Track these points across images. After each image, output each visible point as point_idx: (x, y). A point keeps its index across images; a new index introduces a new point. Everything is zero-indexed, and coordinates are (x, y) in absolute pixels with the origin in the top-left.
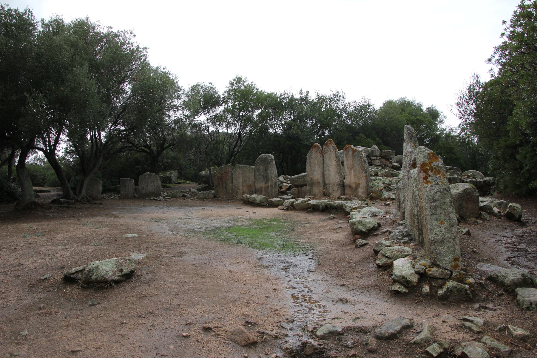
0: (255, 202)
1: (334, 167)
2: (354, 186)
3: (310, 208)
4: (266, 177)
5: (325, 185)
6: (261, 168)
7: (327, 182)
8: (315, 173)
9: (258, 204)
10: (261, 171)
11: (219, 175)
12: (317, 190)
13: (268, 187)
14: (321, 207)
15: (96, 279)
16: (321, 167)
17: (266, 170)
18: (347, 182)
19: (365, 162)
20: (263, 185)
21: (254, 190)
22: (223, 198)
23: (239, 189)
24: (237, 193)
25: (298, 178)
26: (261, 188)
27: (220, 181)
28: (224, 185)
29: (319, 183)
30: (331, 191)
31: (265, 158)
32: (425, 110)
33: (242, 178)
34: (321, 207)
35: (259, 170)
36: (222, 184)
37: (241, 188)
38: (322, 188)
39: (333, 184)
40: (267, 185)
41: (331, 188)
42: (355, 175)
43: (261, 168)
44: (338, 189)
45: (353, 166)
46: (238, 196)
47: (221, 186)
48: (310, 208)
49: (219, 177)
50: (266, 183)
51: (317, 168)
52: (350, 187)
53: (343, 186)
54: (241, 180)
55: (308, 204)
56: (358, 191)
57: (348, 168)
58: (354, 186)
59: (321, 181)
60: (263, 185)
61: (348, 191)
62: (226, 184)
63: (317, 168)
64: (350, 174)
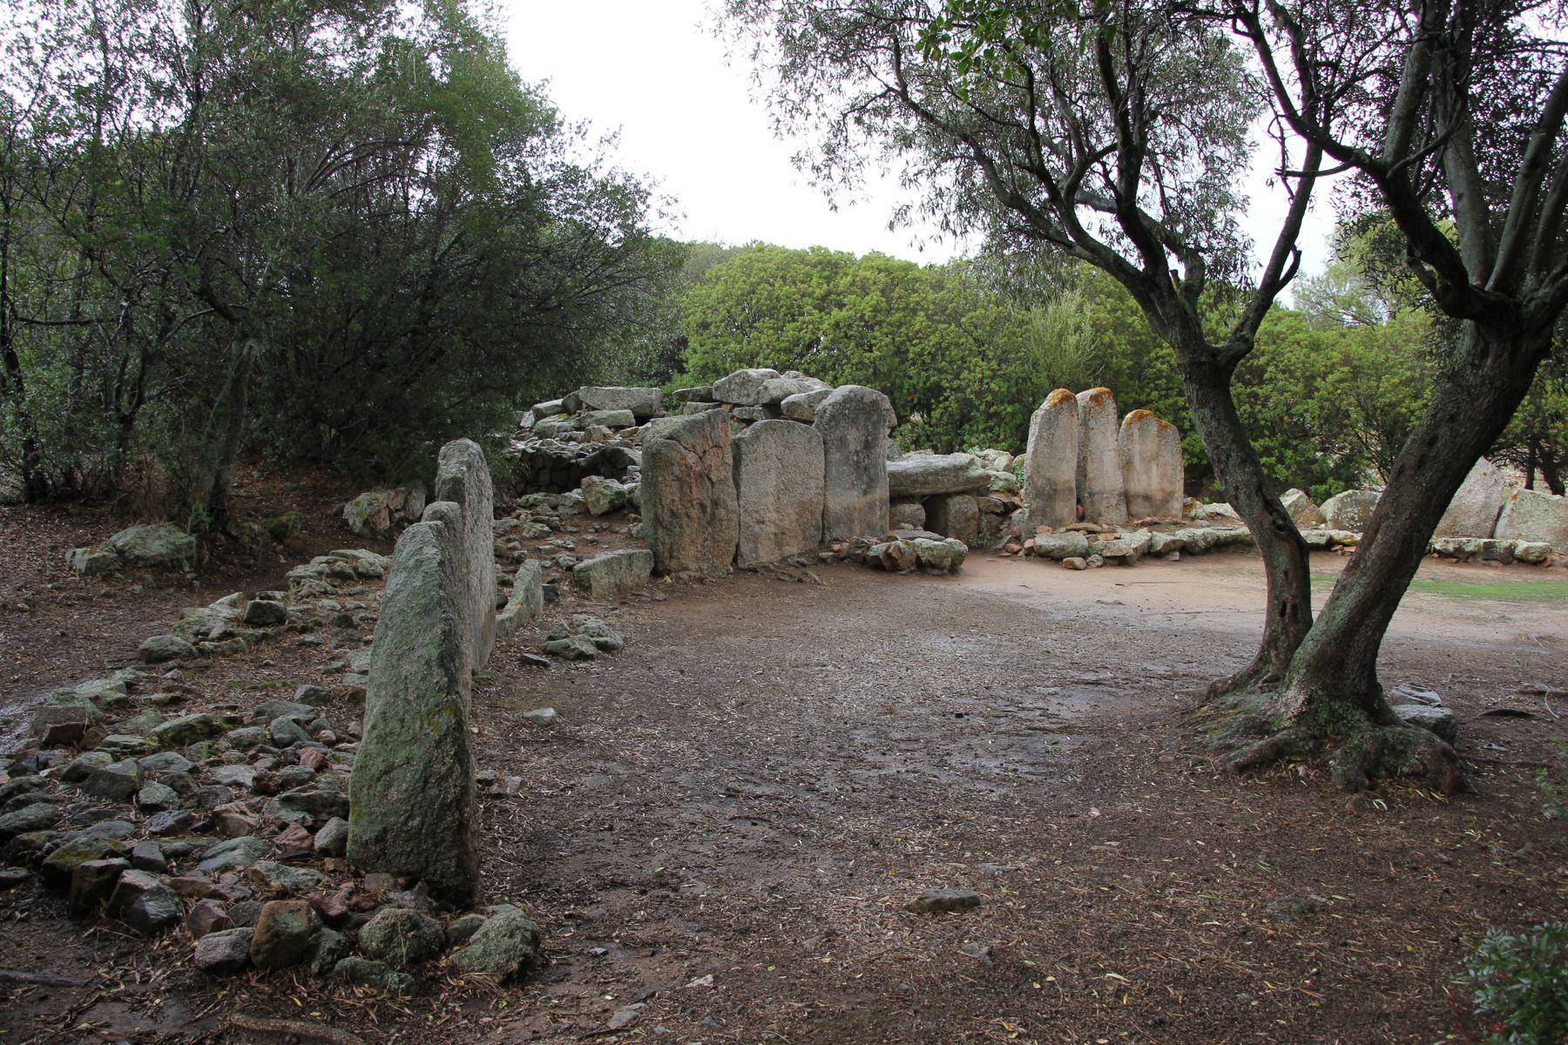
1: (1112, 453)
2: (1159, 496)
8: (1064, 466)
10: (852, 448)
17: (868, 446)
26: (849, 510)
33: (779, 475)
35: (843, 442)
37: (773, 516)
39: (1111, 492)
40: (869, 498)
42: (1162, 476)
45: (1156, 457)
50: (865, 493)
52: (1147, 498)
54: (771, 483)
57: (1142, 459)
58: (1159, 496)
61: (1139, 507)
64: (1148, 472)
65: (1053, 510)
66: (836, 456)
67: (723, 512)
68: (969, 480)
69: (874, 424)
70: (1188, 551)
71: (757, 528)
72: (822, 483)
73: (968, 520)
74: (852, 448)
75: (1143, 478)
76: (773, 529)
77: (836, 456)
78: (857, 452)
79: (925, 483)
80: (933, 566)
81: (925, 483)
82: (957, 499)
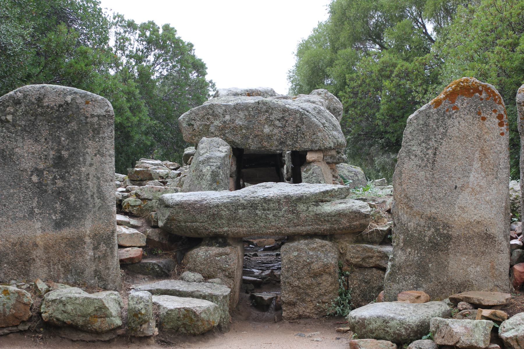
0: (98, 324)
4: (59, 193)
8: (464, 199)
20: (37, 231)
25: (253, 205)
29: (488, 238)
40: (66, 232)
50: (58, 225)
51: (475, 178)
60: (37, 231)
63: (475, 178)
65: (443, 267)
68: (319, 218)
69: (71, 135)
73: (316, 275)
74: (27, 164)
78: (39, 172)
79: (233, 219)
80: (74, 327)
81: (233, 219)
82: (302, 244)
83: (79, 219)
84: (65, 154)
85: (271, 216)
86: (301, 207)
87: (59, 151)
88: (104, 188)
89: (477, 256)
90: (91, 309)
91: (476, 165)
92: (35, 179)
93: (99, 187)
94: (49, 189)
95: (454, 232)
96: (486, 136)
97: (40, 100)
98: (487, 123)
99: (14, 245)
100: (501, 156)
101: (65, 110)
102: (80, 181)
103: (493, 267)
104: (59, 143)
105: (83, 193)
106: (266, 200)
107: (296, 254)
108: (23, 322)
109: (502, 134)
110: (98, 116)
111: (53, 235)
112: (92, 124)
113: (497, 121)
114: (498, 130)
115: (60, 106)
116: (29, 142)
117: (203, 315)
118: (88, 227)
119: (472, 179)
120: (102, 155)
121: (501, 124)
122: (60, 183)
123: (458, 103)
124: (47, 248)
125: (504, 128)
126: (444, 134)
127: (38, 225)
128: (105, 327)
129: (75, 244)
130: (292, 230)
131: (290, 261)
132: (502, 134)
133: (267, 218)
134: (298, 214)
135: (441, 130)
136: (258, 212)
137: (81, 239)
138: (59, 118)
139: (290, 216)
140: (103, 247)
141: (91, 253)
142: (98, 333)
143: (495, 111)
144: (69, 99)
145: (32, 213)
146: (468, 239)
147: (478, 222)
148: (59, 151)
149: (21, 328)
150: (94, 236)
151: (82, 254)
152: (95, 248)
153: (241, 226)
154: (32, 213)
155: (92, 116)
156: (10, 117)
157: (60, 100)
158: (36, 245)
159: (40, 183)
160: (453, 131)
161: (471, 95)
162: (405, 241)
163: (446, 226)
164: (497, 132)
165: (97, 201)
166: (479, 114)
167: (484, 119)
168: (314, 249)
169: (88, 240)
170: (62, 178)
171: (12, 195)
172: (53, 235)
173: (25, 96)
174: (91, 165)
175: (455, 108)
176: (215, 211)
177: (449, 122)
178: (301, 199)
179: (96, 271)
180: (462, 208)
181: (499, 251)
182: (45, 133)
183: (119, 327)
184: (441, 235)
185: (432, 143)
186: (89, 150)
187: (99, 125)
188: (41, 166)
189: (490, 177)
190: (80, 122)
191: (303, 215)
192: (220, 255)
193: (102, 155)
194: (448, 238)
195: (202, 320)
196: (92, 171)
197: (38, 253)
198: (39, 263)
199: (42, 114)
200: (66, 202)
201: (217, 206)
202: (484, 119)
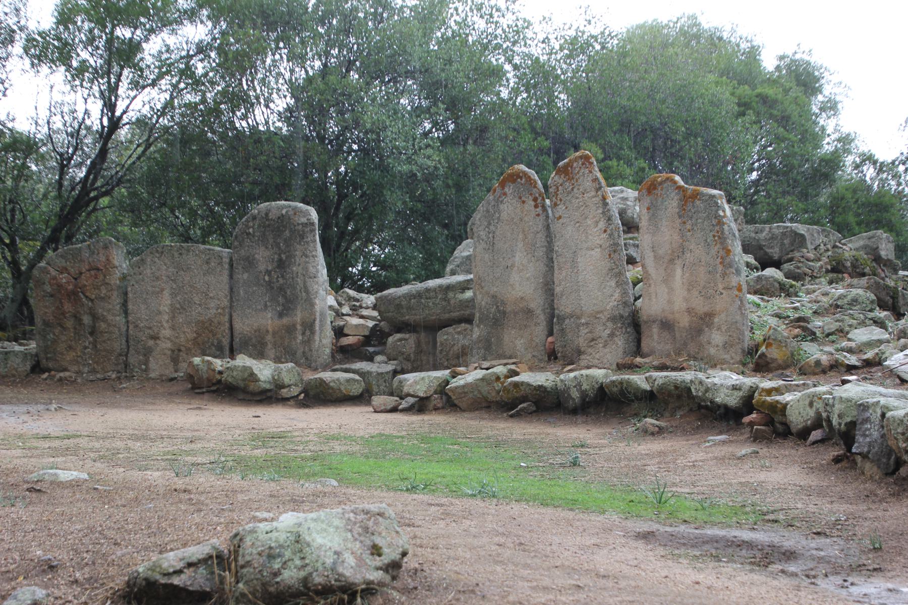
0: (252, 387)
1: (596, 253)
2: (684, 321)
3: (524, 399)
4: (281, 289)
5: (553, 320)
6: (263, 256)
7: (565, 306)
8: (515, 277)
9: (265, 391)
10: (262, 267)
11: (64, 279)
12: (516, 340)
13: (290, 330)
14: (575, 394)
15: (305, 581)
16: (540, 253)
17: (281, 265)
18: (652, 306)
19: (734, 235)
20: (268, 320)
21: (226, 342)
22: (79, 373)
23: (155, 338)
24: (148, 352)
25: (419, 295)
27: (68, 307)
28: (87, 319)
29: (529, 312)
30: (582, 342)
31: (281, 217)
32: (769, 63)
33: (173, 295)
34: (575, 394)
35: (250, 262)
36: (77, 318)
37: (166, 332)
38: (539, 330)
39: (595, 316)
40: (285, 320)
41: (584, 331)
42: (690, 286)
43: (263, 256)
44: (612, 335)
46: (152, 364)
47: (70, 323)
48: (524, 399)
49: (60, 286)
50: (281, 315)
51: (520, 257)
52: (667, 325)
53: (634, 325)
55: (516, 385)
56: (704, 338)
59: (537, 303)
60: (268, 320)
61: (653, 339)
62: (95, 317)
63: (520, 257)
64: (667, 280)
66: (243, 276)
67: (103, 325)
70: (548, 405)
71: (151, 343)
72: (226, 302)
74: (262, 267)
75: (662, 290)
76: (169, 345)
77: (243, 276)
78: (268, 272)
83: (293, 310)
84: (283, 256)
85: (431, 304)
86: (451, 295)
87: (280, 255)
88: (308, 284)
89: (520, 329)
90: (246, 375)
91: (520, 245)
92: (267, 278)
93: (305, 283)
94: (276, 285)
95: (509, 309)
96: (526, 219)
97: (267, 214)
98: (526, 206)
99: (255, 331)
100: (539, 235)
101: (282, 222)
102: (293, 278)
103: (532, 340)
104: (280, 248)
105: (295, 288)
106: (428, 290)
107: (445, 337)
108: (214, 384)
109: (538, 215)
110: (302, 224)
111: (278, 322)
112: (299, 232)
113: (533, 203)
114: (533, 212)
115: (279, 218)
116: (263, 248)
117: (332, 384)
118: (298, 316)
119: (517, 258)
120: (307, 256)
121: (536, 206)
122: (281, 281)
123: (506, 190)
124: (274, 333)
125: (539, 210)
126: (499, 218)
127: (270, 315)
128: (256, 390)
129: (290, 330)
130: (447, 316)
131: (442, 344)
132: (538, 215)
133: (428, 306)
134: (449, 301)
135: (497, 215)
136: (423, 301)
137: (294, 326)
138: (278, 228)
139: (444, 303)
140: (308, 333)
141: (300, 338)
142: (253, 394)
143: (531, 194)
144: (284, 212)
145: (266, 306)
146: (516, 314)
147: (522, 298)
148: (280, 255)
149: (212, 388)
150: (303, 324)
151: (295, 338)
152: (303, 334)
153: (415, 314)
154: (266, 306)
155: (298, 224)
156: (251, 230)
157: (278, 214)
158: (268, 331)
159: (270, 281)
160: (504, 216)
161: (514, 181)
162: (480, 319)
163: (503, 303)
164: (533, 213)
165: (304, 294)
166: (520, 198)
167: (524, 202)
168: (459, 333)
169: (299, 327)
170: (283, 276)
171: (254, 292)
172: (278, 322)
173: (259, 212)
174: (299, 265)
175: (505, 194)
176: (397, 302)
177: (501, 207)
178: (449, 288)
179: (304, 352)
180: (512, 286)
181: (537, 324)
182: (271, 241)
183: (270, 390)
184: (499, 311)
185: (492, 228)
186: (297, 253)
187: (303, 231)
188: (270, 268)
189: (530, 255)
190: (291, 231)
191: (452, 302)
192: (400, 340)
193: (307, 256)
194: (504, 313)
195: (332, 388)
196: (300, 271)
197: (269, 338)
198: (270, 346)
199: (269, 226)
200: (285, 296)
201: (399, 297)
202: (524, 202)
